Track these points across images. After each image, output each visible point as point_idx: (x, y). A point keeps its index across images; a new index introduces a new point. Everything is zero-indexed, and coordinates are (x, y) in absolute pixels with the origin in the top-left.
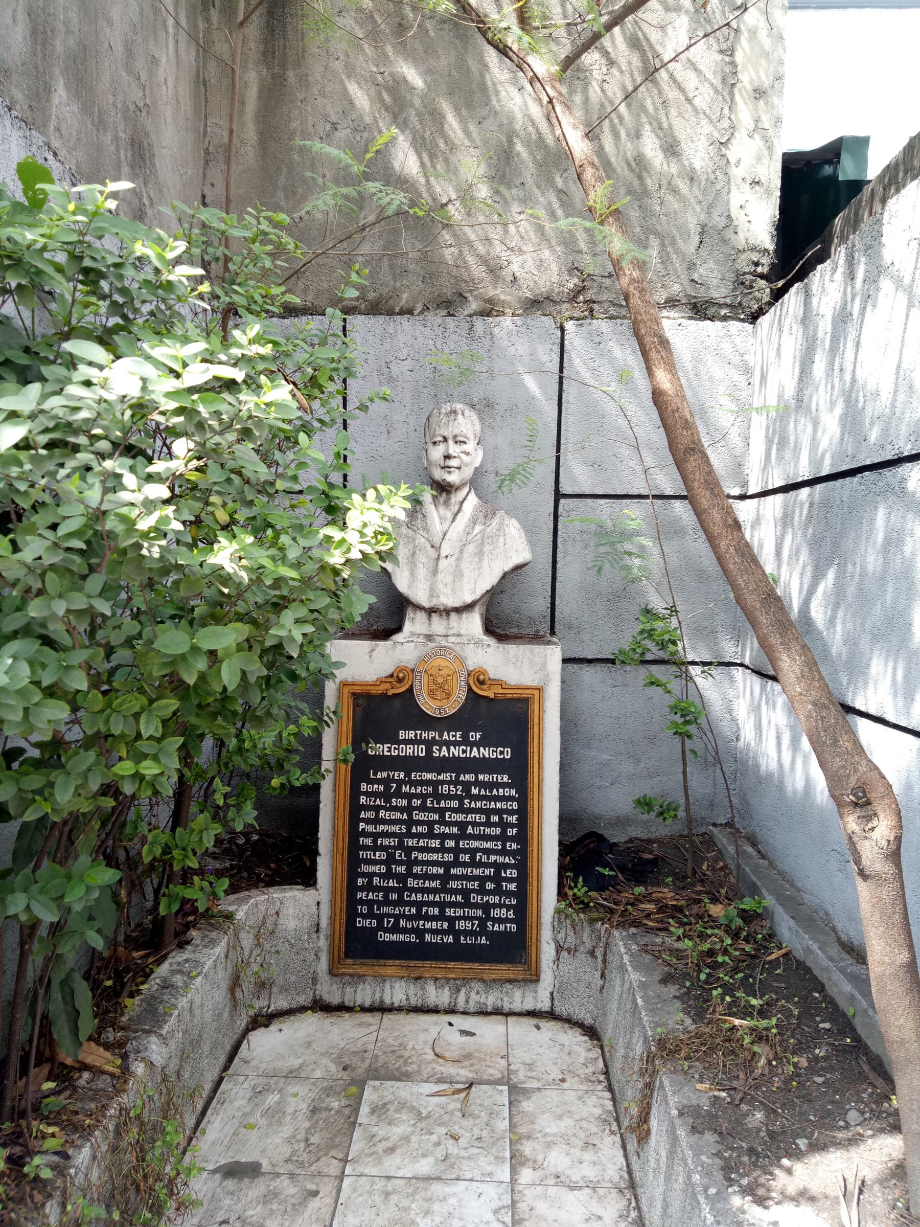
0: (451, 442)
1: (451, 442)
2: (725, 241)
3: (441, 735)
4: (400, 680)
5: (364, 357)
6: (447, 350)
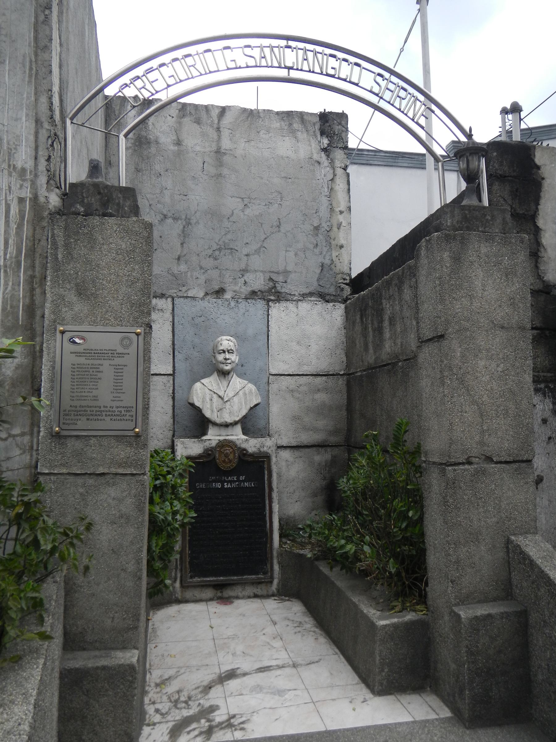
0: (227, 353)
1: (227, 353)
2: (331, 269)
3: (227, 478)
4: (209, 455)
6: (219, 313)
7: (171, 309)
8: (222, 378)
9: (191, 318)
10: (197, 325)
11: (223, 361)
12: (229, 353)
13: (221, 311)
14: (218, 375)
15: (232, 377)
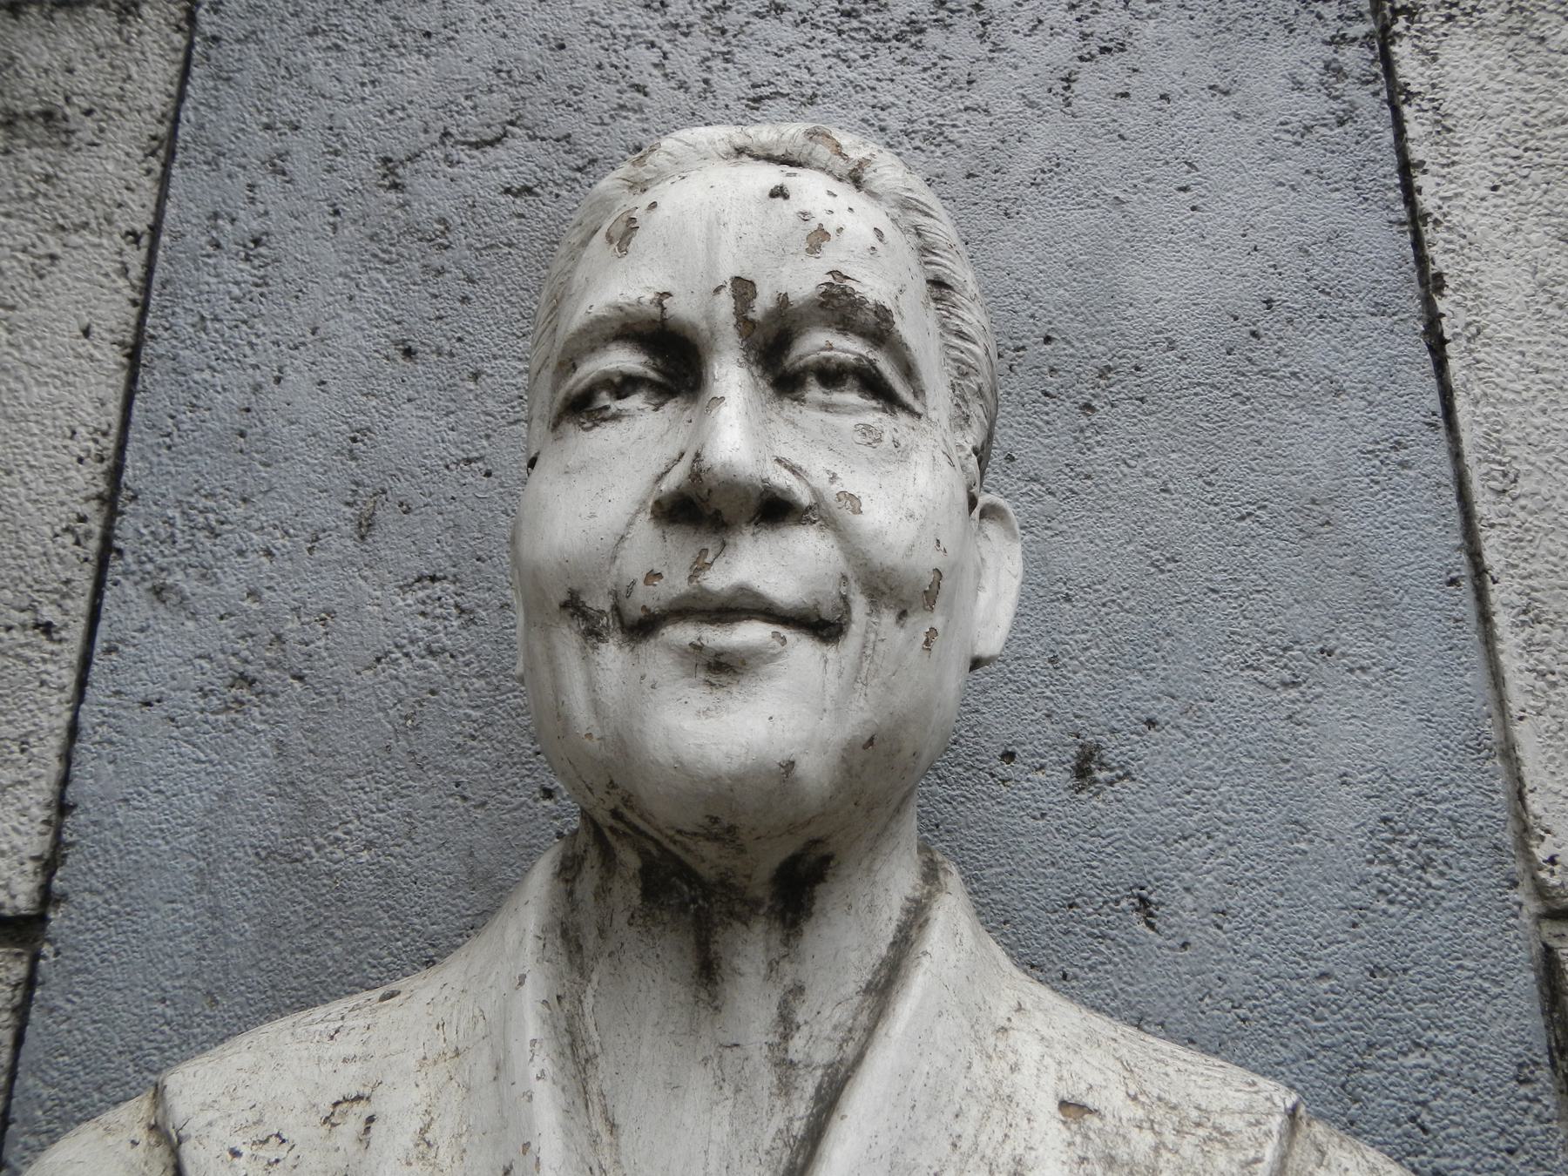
0: (731, 377)
1: (731, 377)
5: (265, 144)
7: (160, 102)
8: (650, 981)
9: (365, 168)
10: (439, 236)
11: (656, 562)
12: (782, 374)
13: (763, 66)
14: (570, 940)
15: (884, 986)
